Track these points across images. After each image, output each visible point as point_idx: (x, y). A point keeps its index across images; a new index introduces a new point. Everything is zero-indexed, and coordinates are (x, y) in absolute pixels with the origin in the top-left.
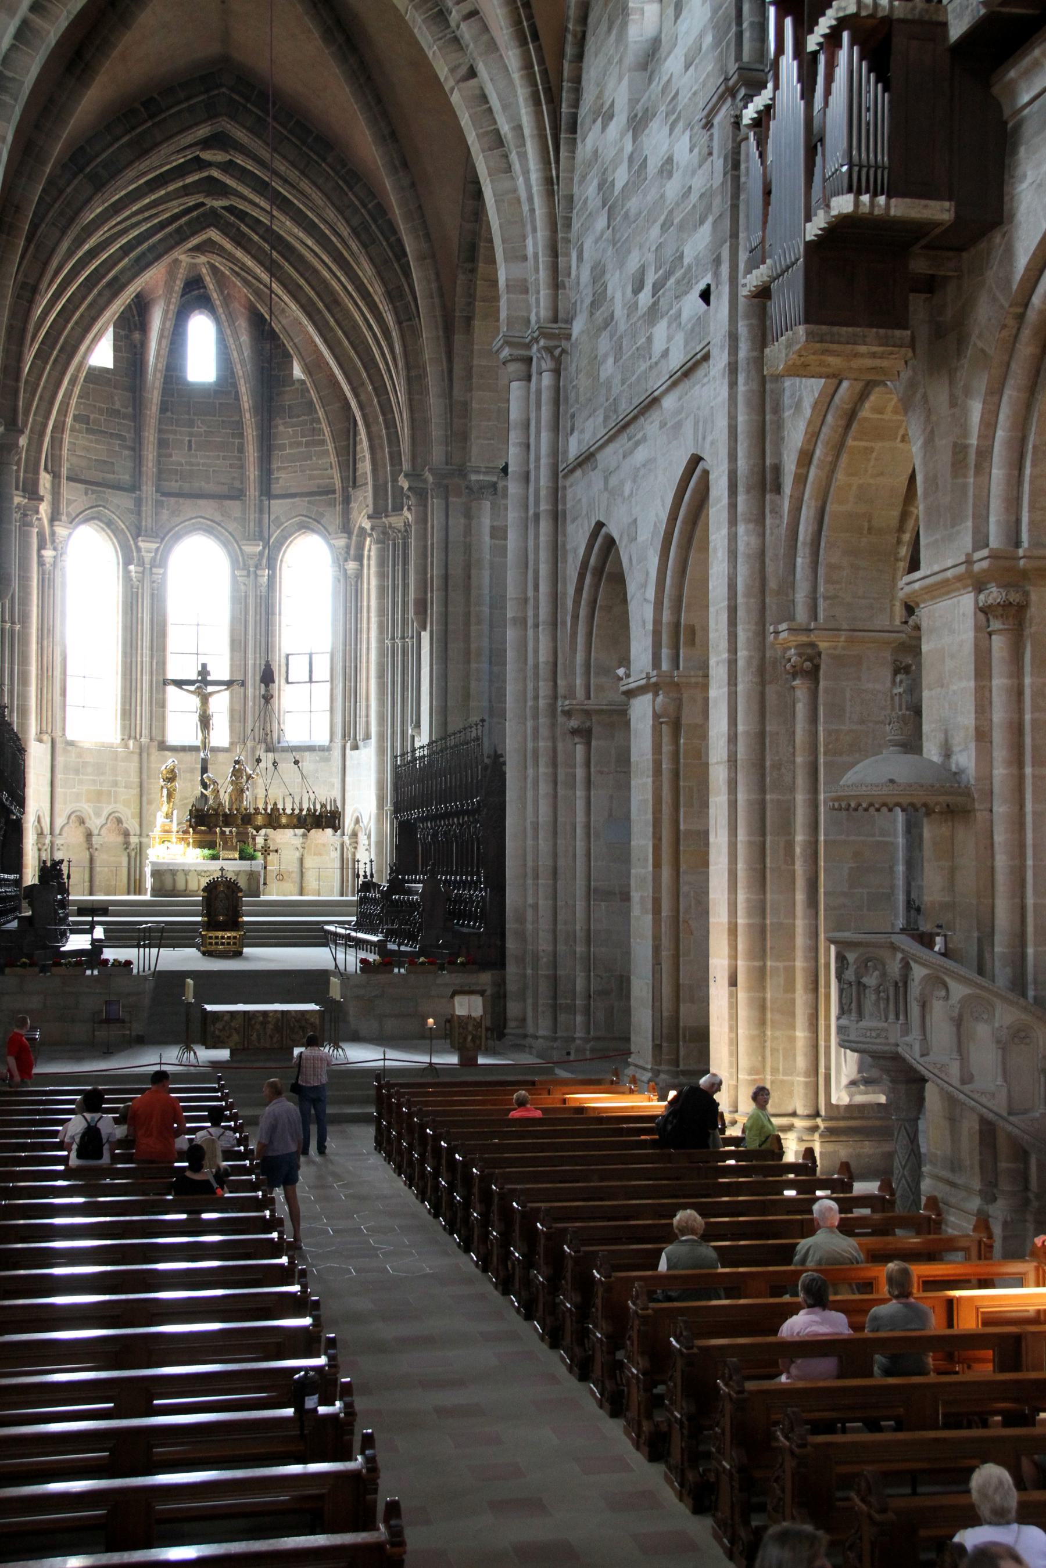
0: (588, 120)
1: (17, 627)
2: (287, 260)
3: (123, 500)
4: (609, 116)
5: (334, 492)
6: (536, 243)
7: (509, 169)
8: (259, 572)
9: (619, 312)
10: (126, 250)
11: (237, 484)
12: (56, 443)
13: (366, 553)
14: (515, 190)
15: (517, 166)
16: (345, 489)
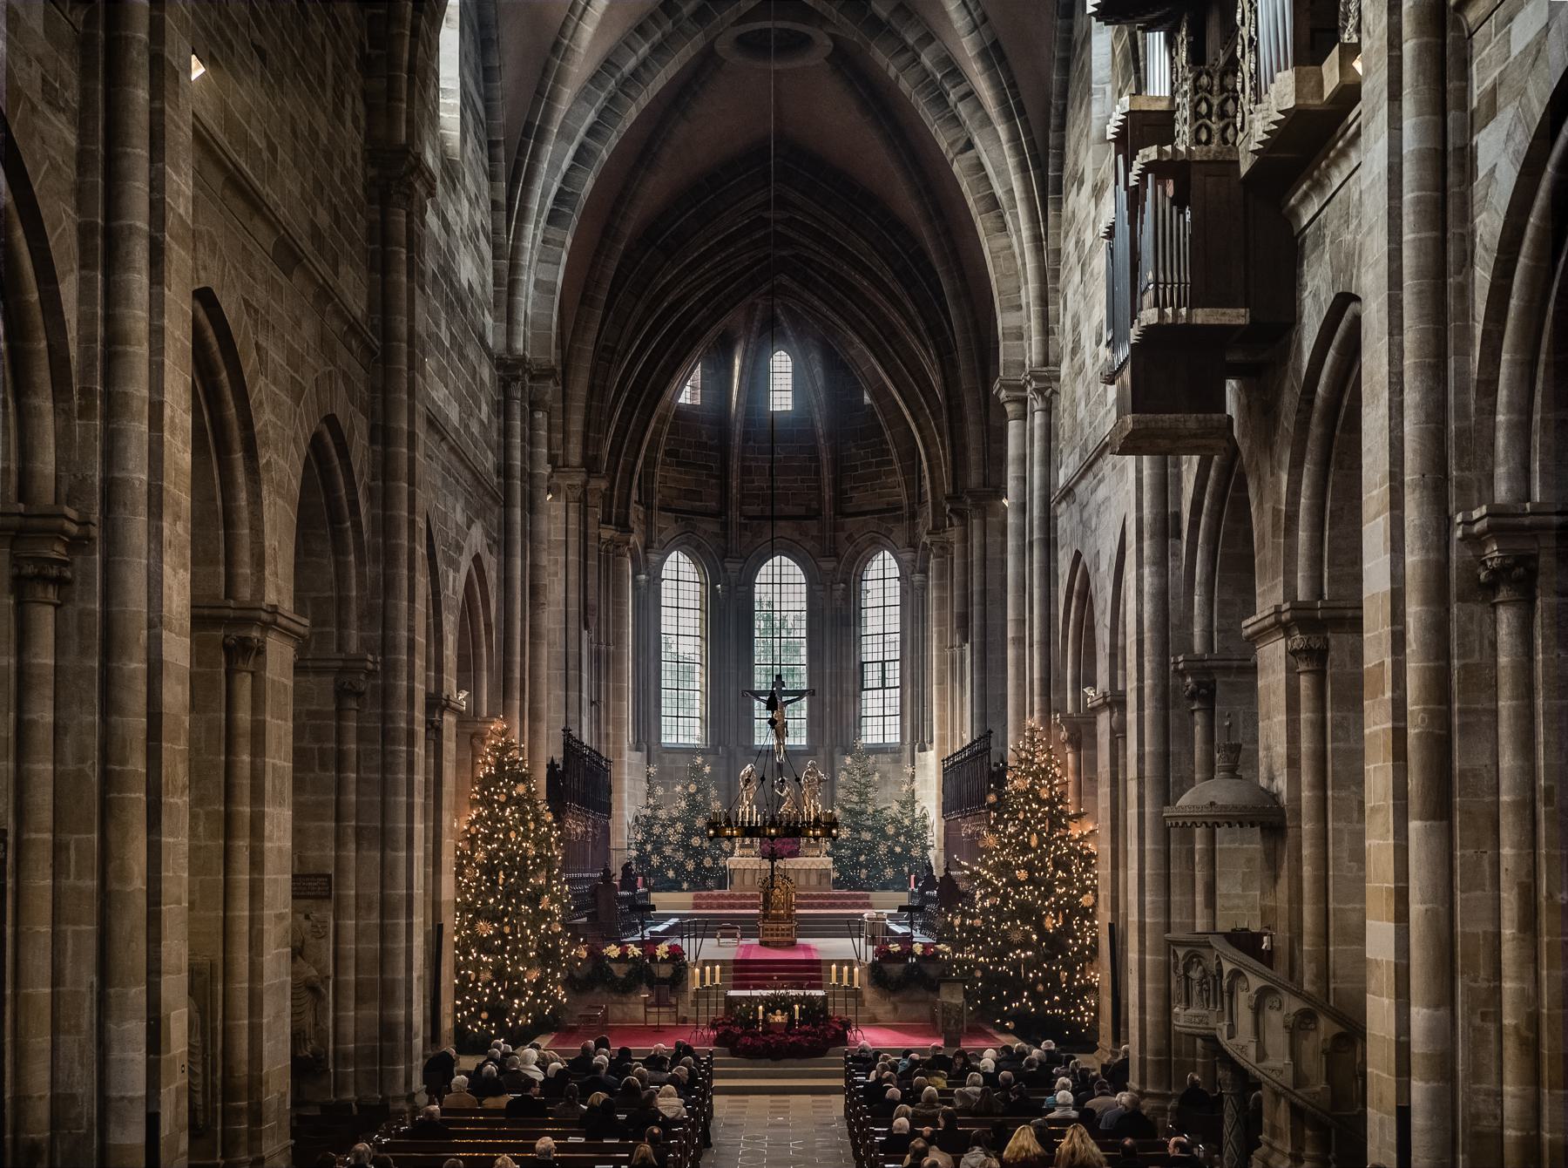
0: (1069, 184)
1: (612, 648)
2: (849, 299)
3: (712, 526)
4: (1081, 183)
5: (900, 508)
6: (1029, 293)
7: (1004, 228)
8: (834, 587)
9: (1089, 362)
11: (814, 505)
12: (648, 476)
14: (1010, 247)
15: (1010, 225)
16: (911, 506)
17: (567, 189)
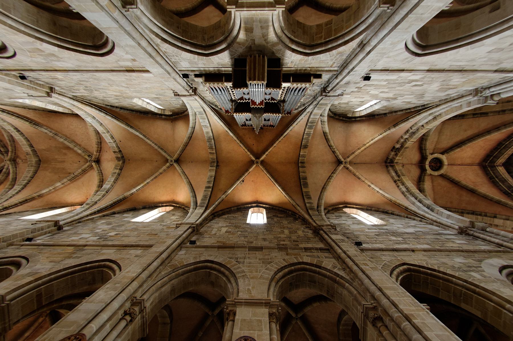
6: (455, 104)
7: (440, 114)
14: (445, 112)
17: (426, 206)
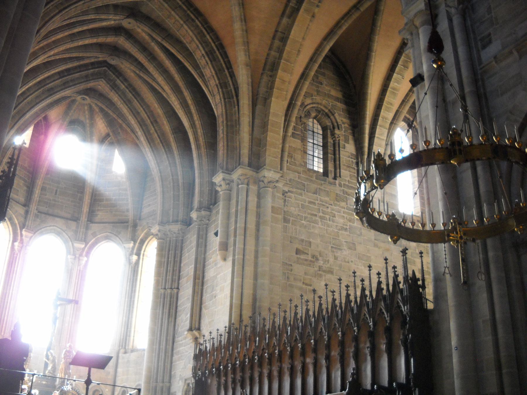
5: (127, 222)
8: (81, 258)
10: (61, 74)
13: (142, 252)
